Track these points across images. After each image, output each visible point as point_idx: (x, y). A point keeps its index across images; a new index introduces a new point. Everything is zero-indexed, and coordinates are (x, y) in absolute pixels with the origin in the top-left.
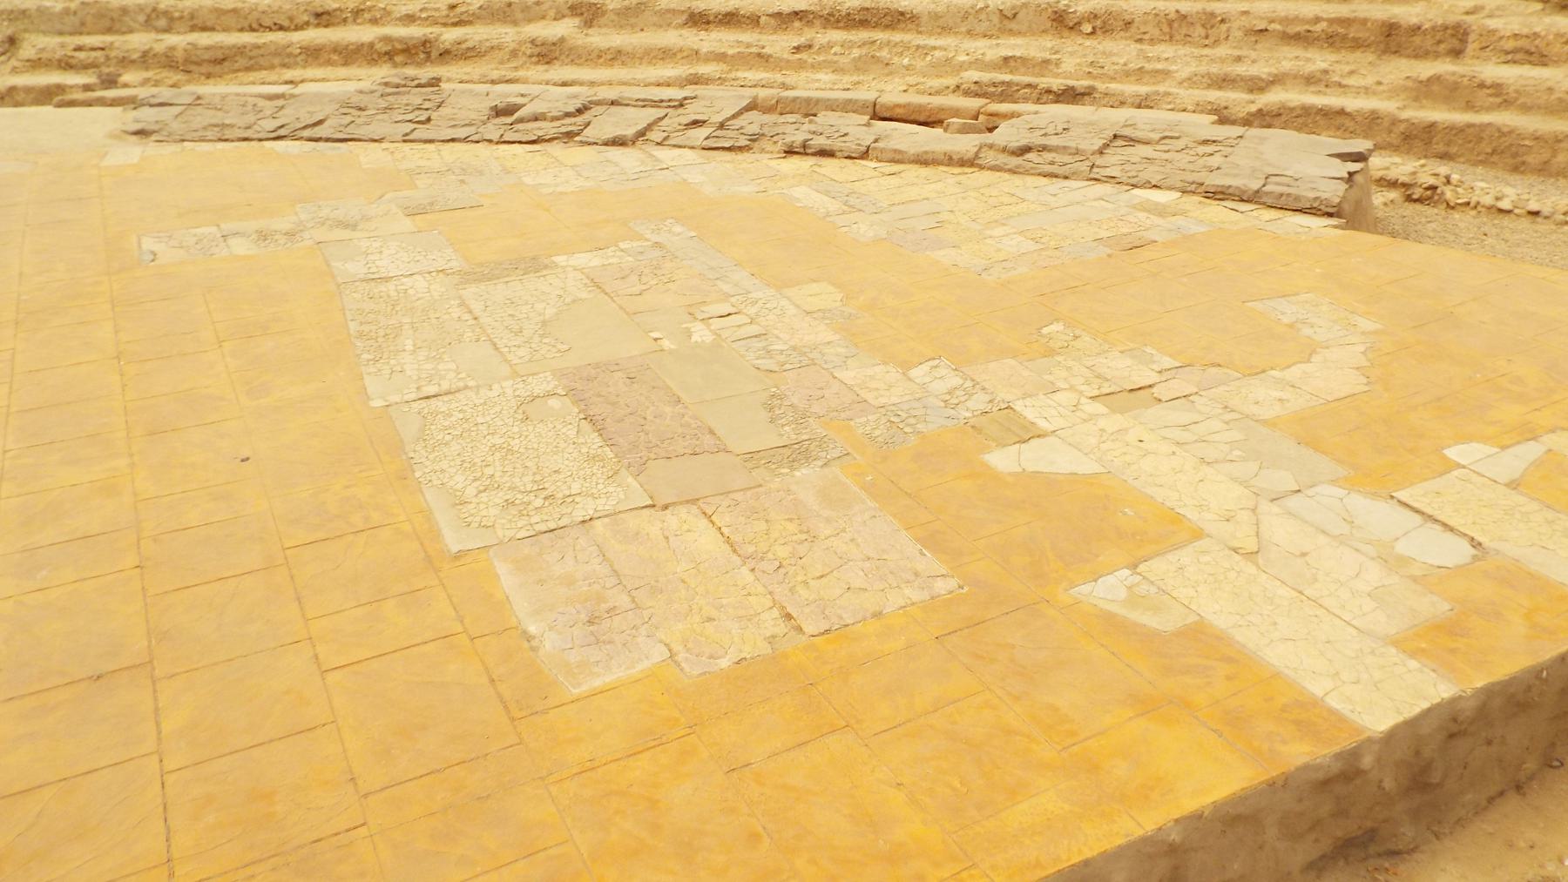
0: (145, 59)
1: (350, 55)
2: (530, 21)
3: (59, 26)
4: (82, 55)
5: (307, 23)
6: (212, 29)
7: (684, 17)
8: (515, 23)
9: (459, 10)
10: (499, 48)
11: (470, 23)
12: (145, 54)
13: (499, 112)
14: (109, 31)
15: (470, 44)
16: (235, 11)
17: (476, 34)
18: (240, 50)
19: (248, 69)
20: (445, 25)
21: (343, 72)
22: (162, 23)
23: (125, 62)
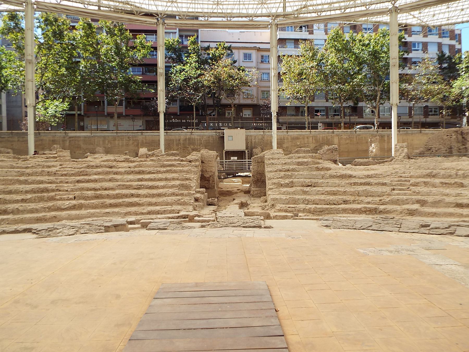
0: (304, 211)
1: (354, 211)
2: (404, 204)
3: (283, 202)
4: (290, 209)
5: (342, 203)
6: (318, 204)
7: (455, 204)
8: (399, 205)
9: (382, 201)
10: (396, 211)
11: (386, 204)
12: (304, 209)
13: (423, 226)
14: (294, 204)
15: (388, 210)
16: (324, 200)
17: (389, 207)
18: (327, 209)
19: (328, 214)
20: (378, 205)
21: (358, 215)
22: (306, 202)
23: (299, 211)
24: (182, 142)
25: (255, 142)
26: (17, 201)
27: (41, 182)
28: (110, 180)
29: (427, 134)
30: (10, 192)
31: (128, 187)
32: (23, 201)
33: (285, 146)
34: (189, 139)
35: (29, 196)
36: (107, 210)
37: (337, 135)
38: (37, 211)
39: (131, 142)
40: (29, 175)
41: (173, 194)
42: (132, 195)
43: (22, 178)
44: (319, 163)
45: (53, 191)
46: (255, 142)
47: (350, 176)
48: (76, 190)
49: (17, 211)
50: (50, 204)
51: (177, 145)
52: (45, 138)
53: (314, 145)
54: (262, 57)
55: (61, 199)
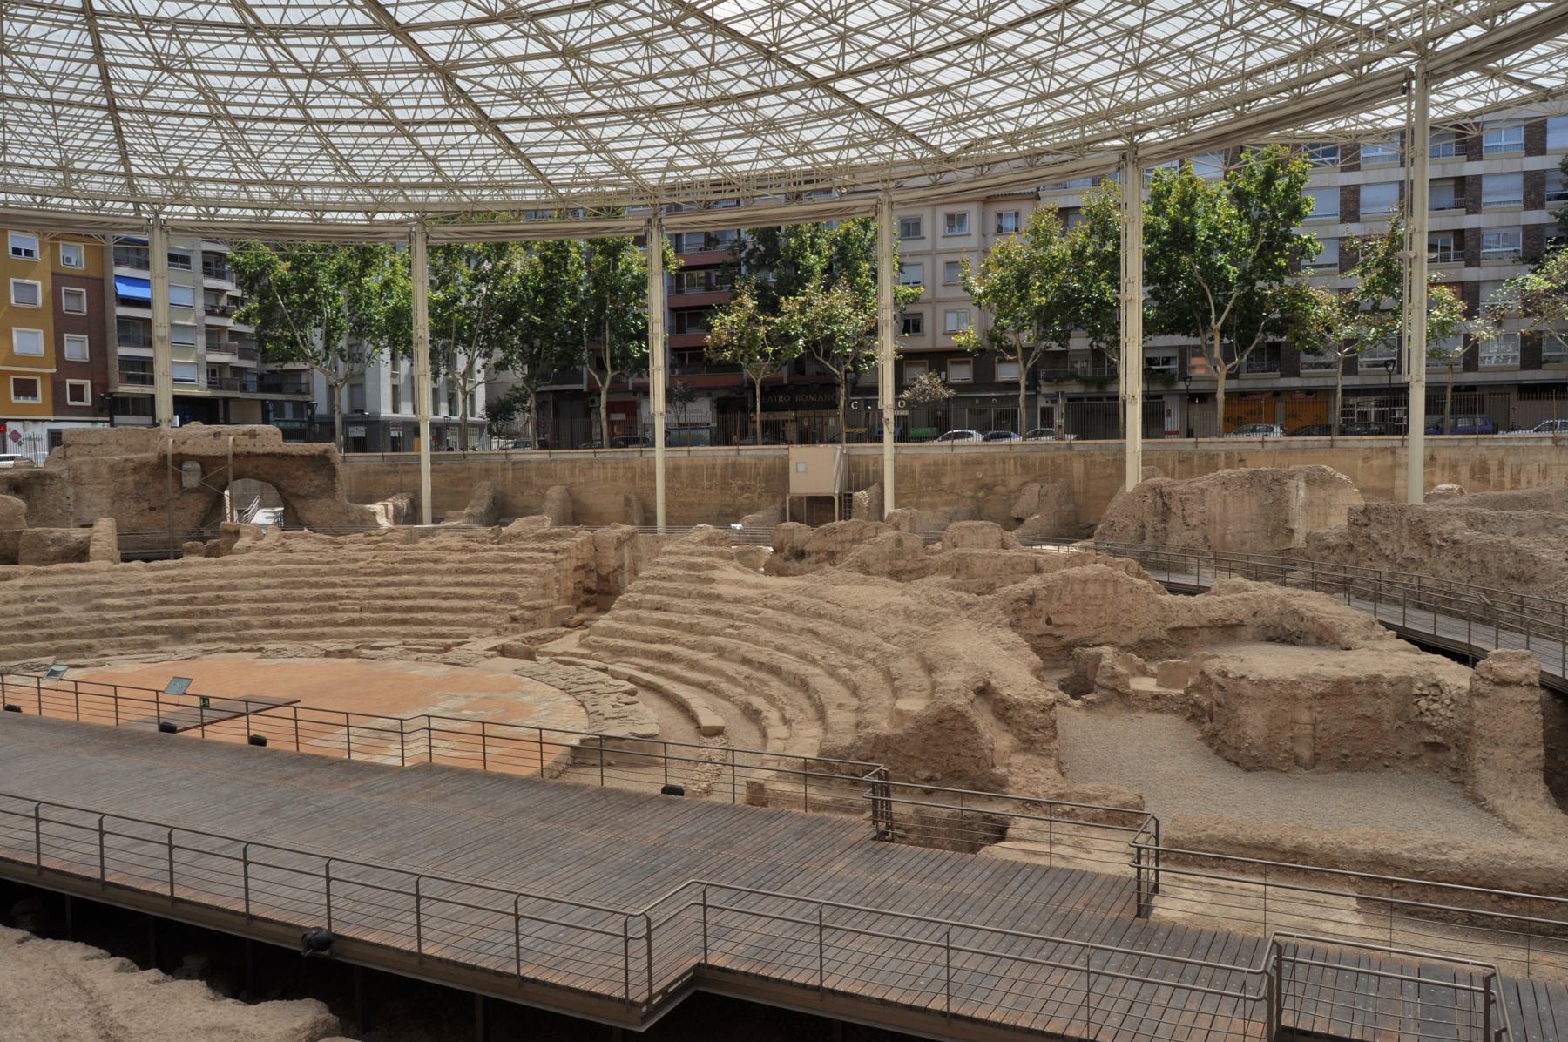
24: (718, 471)
25: (876, 472)
26: (295, 612)
27: (334, 585)
28: (419, 584)
29: (1350, 450)
30: (294, 599)
31: (434, 596)
32: (303, 611)
33: (946, 480)
34: (734, 465)
35: (311, 604)
36: (382, 629)
37: (1082, 455)
38: (311, 625)
39: (621, 471)
40: (326, 574)
41: (483, 610)
42: (431, 609)
43: (313, 579)
44: (713, 568)
45: (342, 598)
46: (876, 472)
47: (719, 597)
48: (370, 598)
49: (289, 625)
50: (326, 617)
51: (710, 477)
52: (473, 465)
53: (1020, 480)
54: (1000, 215)
55: (344, 611)
